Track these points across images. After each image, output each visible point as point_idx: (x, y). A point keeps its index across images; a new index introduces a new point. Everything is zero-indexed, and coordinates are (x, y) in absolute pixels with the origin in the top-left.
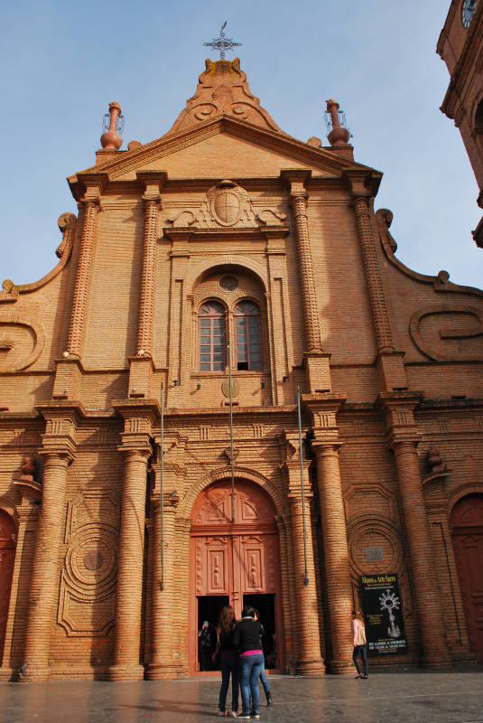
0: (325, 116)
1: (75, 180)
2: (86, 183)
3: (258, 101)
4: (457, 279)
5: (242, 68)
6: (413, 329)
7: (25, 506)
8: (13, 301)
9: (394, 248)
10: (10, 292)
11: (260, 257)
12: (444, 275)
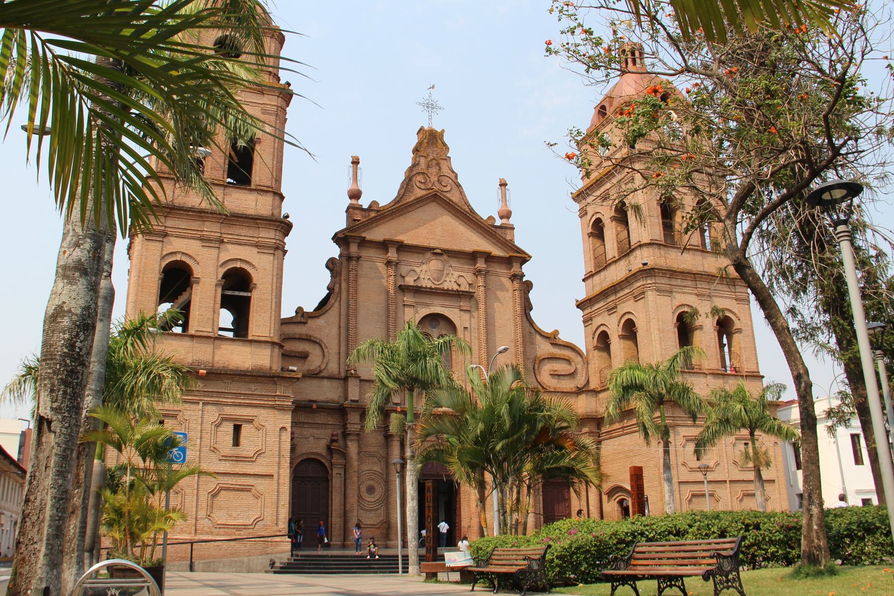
0: (498, 193)
1: (341, 236)
3: (456, 176)
4: (564, 337)
5: (446, 139)
6: (536, 368)
7: (336, 459)
8: (305, 323)
9: (531, 309)
11: (457, 311)
12: (556, 332)
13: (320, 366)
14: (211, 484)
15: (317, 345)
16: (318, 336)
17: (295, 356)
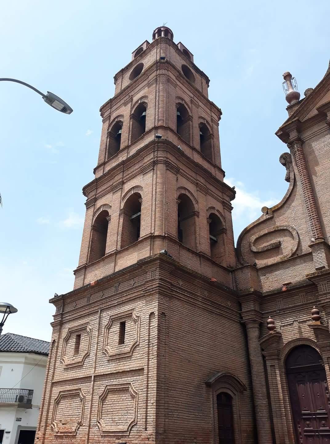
2: (287, 131)
10: (267, 213)
13: (292, 250)
14: (101, 386)
15: (286, 232)
16: (286, 223)
17: (268, 250)
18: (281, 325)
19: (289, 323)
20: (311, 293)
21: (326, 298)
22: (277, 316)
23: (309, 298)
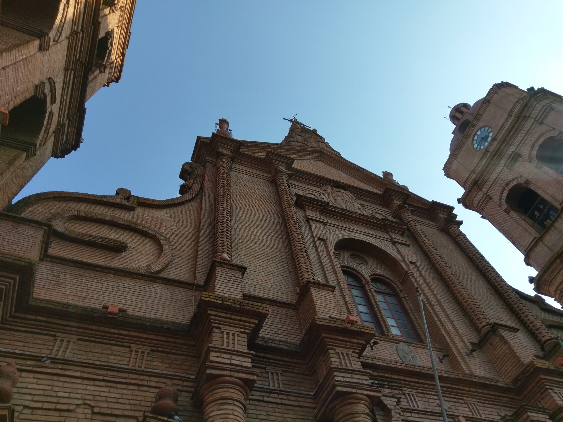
18: (27, 403)
19: (59, 406)
20: (166, 355)
21: (228, 361)
22: (32, 375)
23: (154, 363)
